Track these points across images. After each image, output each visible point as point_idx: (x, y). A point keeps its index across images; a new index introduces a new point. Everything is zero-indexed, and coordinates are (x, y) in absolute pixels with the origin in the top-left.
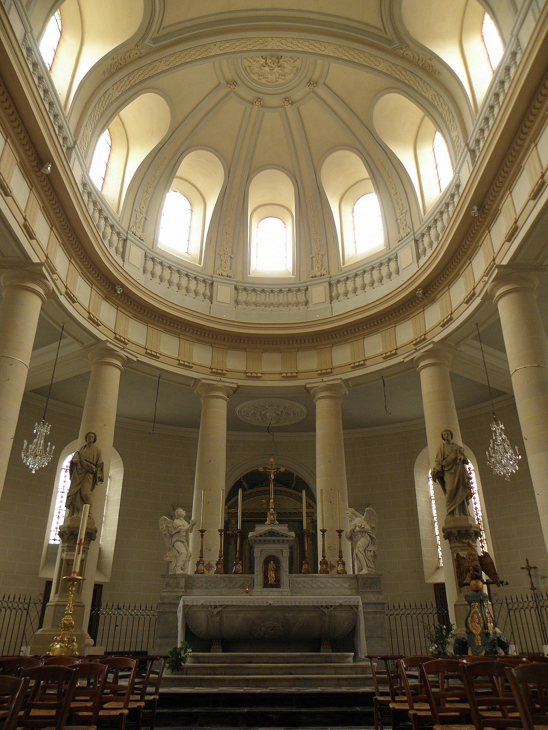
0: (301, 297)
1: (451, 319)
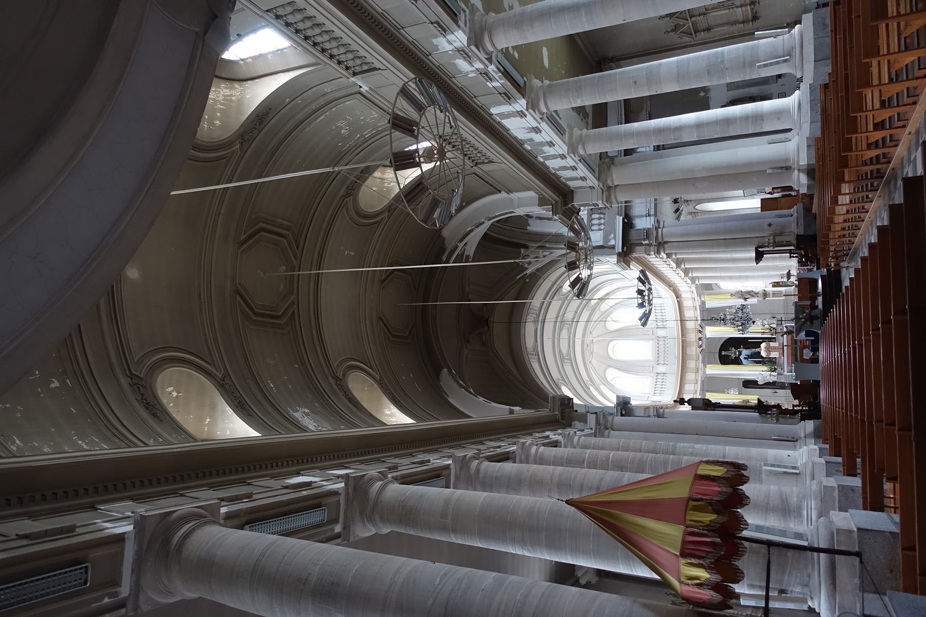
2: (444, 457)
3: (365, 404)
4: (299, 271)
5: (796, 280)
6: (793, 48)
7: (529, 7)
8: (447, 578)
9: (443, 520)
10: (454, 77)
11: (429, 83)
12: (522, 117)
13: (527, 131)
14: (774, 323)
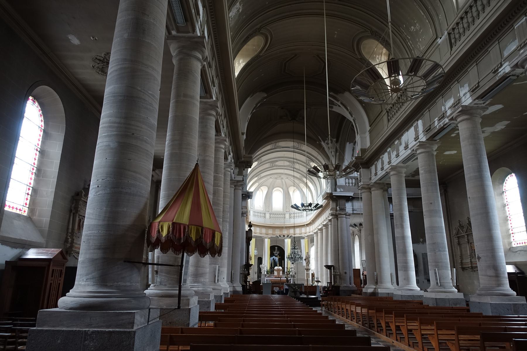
2: (217, 95)
3: (245, 47)
4: (325, 2)
5: (315, 285)
6: (444, 288)
7: (482, 143)
8: (152, 97)
9: (182, 95)
10: (442, 98)
11: (440, 82)
12: (415, 139)
13: (406, 142)
14: (292, 273)
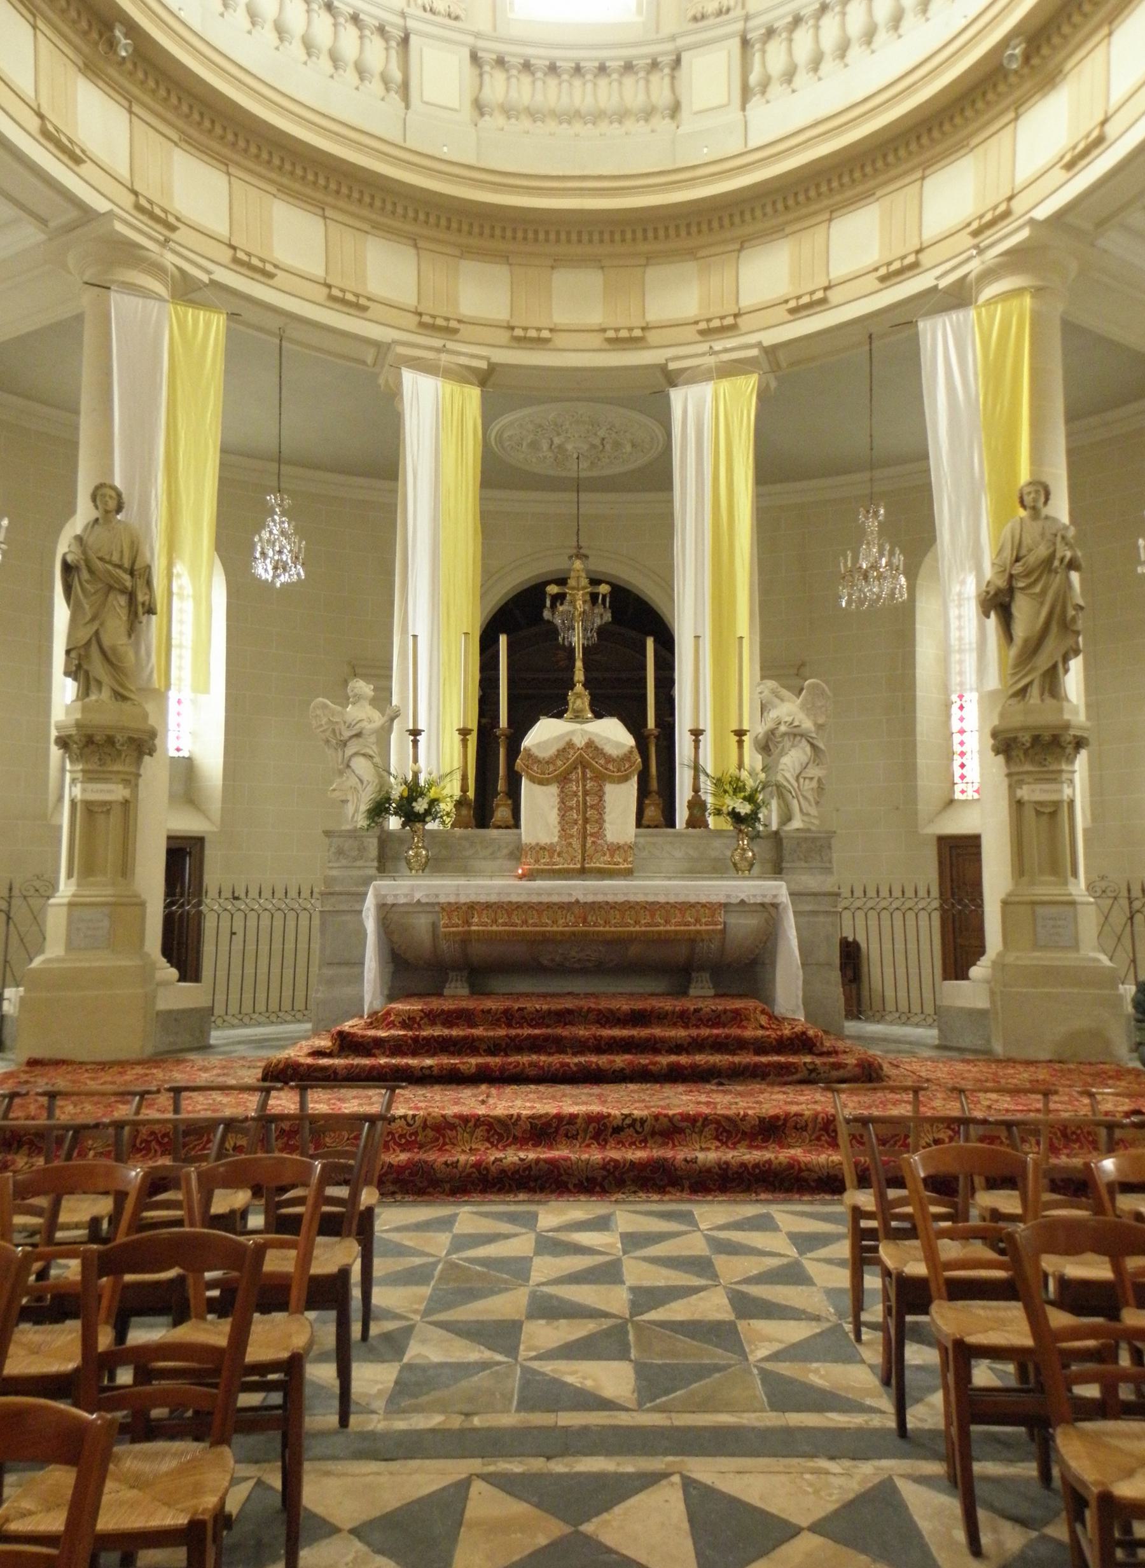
0: (660, 90)
1: (1100, 140)
14: (787, 818)
